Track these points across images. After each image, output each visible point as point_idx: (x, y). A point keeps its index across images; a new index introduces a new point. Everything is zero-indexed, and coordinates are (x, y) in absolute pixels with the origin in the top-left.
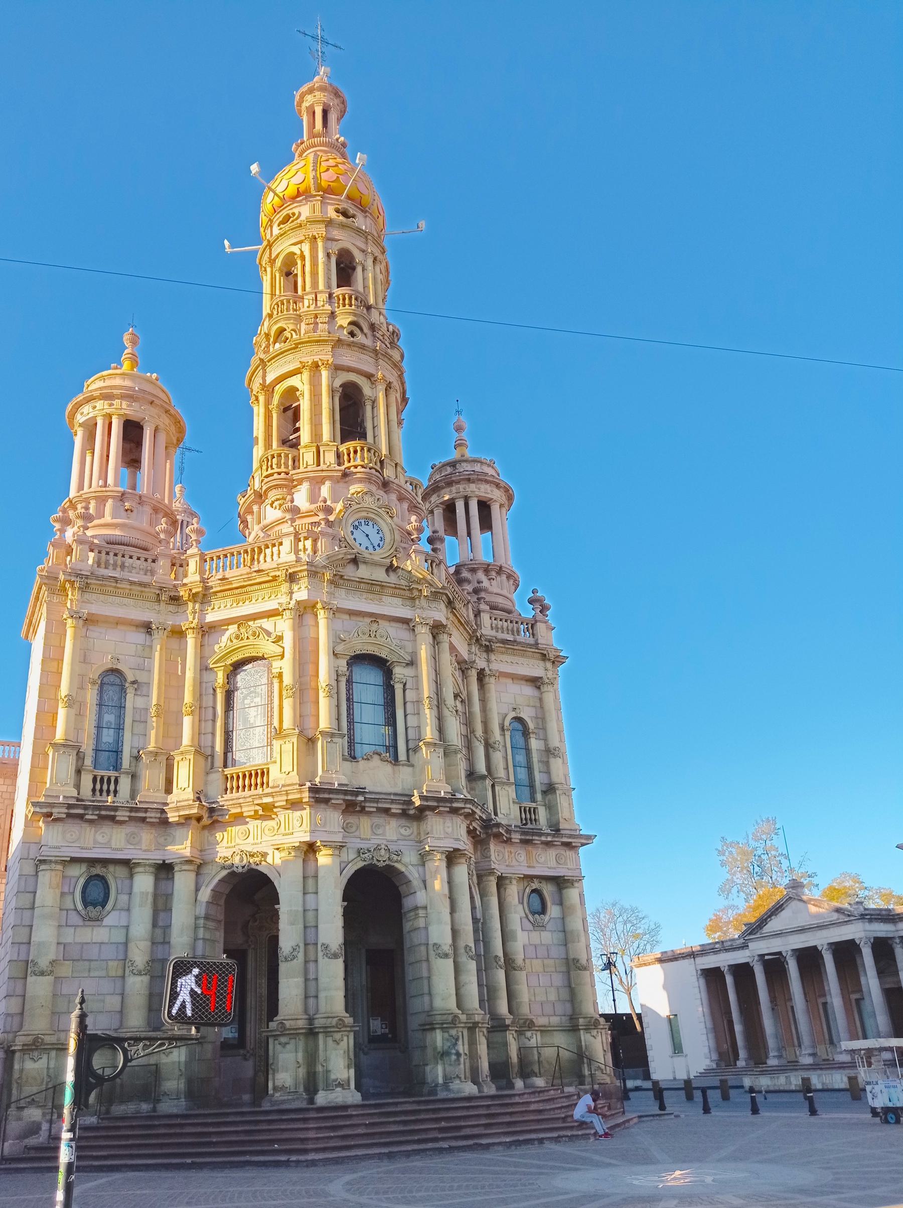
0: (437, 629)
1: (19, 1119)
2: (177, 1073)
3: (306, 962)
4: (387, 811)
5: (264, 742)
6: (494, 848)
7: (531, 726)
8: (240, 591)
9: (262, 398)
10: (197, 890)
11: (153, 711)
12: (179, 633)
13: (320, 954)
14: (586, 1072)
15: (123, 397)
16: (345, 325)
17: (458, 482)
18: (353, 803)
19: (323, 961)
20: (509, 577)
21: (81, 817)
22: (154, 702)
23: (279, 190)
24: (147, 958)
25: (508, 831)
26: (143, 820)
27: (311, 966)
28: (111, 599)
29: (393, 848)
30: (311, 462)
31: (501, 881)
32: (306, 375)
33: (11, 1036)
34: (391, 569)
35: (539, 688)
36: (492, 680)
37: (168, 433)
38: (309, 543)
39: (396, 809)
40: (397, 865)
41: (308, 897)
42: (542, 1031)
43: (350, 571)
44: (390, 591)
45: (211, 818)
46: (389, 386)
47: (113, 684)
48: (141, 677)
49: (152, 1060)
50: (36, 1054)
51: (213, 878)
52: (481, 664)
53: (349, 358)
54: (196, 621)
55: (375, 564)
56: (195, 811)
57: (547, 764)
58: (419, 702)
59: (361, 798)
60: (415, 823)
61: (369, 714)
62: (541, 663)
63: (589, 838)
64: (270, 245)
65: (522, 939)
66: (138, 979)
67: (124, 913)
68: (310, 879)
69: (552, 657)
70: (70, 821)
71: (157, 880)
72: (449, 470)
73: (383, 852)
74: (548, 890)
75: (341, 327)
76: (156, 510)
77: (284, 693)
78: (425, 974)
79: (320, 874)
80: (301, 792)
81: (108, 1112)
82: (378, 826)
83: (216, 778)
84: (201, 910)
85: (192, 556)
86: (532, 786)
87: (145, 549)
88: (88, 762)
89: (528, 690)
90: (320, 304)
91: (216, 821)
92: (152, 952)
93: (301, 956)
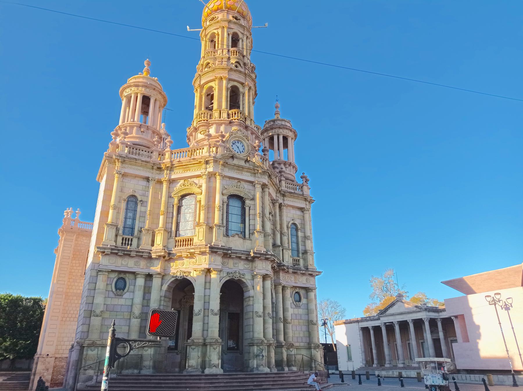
0: (264, 186)
1: (84, 374)
2: (150, 358)
3: (204, 316)
4: (240, 257)
5: (192, 227)
6: (281, 274)
7: (299, 227)
8: (185, 167)
9: (199, 90)
10: (162, 285)
11: (148, 212)
12: (160, 182)
13: (210, 313)
14: (313, 366)
15: (143, 86)
16: (234, 63)
17: (275, 128)
18: (227, 254)
19: (211, 316)
20: (294, 167)
21: (116, 254)
22: (149, 209)
23: (210, 7)
24: (140, 312)
25: (288, 268)
26: (142, 256)
27: (206, 318)
28: (134, 167)
29: (241, 272)
30: (217, 117)
31: (284, 288)
32: (217, 82)
33: (83, 340)
34: (247, 161)
35: (303, 212)
36: (285, 208)
37: (160, 101)
38: (214, 149)
39: (243, 257)
40: (243, 279)
41: (206, 290)
42: (297, 349)
43: (230, 161)
44: (246, 170)
45: (169, 257)
46: (250, 88)
47: (133, 201)
48: (144, 199)
49: (140, 353)
50: (93, 348)
51: (169, 281)
52: (280, 201)
53: (235, 76)
54: (167, 178)
55: (241, 159)
56: (163, 254)
57: (305, 242)
58: (255, 215)
59: (230, 252)
60: (251, 263)
61: (235, 219)
62: (304, 202)
63: (320, 272)
64: (205, 29)
65: (291, 311)
66: (137, 320)
67: (131, 294)
68: (207, 283)
69: (309, 199)
70: (112, 255)
71: (146, 280)
72: (272, 123)
73: (237, 274)
74: (302, 292)
75: (232, 63)
76: (154, 132)
77: (201, 208)
78: (251, 323)
79: (212, 281)
80: (206, 248)
81: (121, 373)
82: (236, 264)
83: (172, 241)
84: (163, 294)
85: (167, 151)
86: (298, 251)
87: (149, 148)
88: (121, 232)
89: (299, 213)
90: (224, 53)
91: (170, 259)
92: (142, 309)
93: (202, 313)
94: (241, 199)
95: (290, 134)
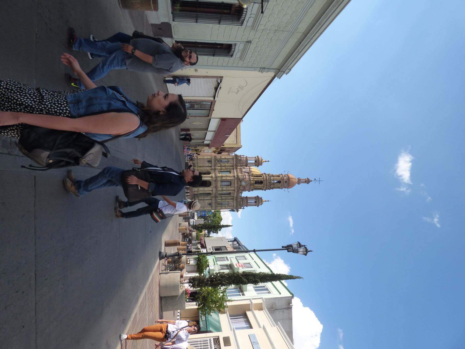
8: (237, 171)
18: (216, 181)
31: (211, 200)
65: (207, 201)
94: (230, 185)
95: (257, 203)
